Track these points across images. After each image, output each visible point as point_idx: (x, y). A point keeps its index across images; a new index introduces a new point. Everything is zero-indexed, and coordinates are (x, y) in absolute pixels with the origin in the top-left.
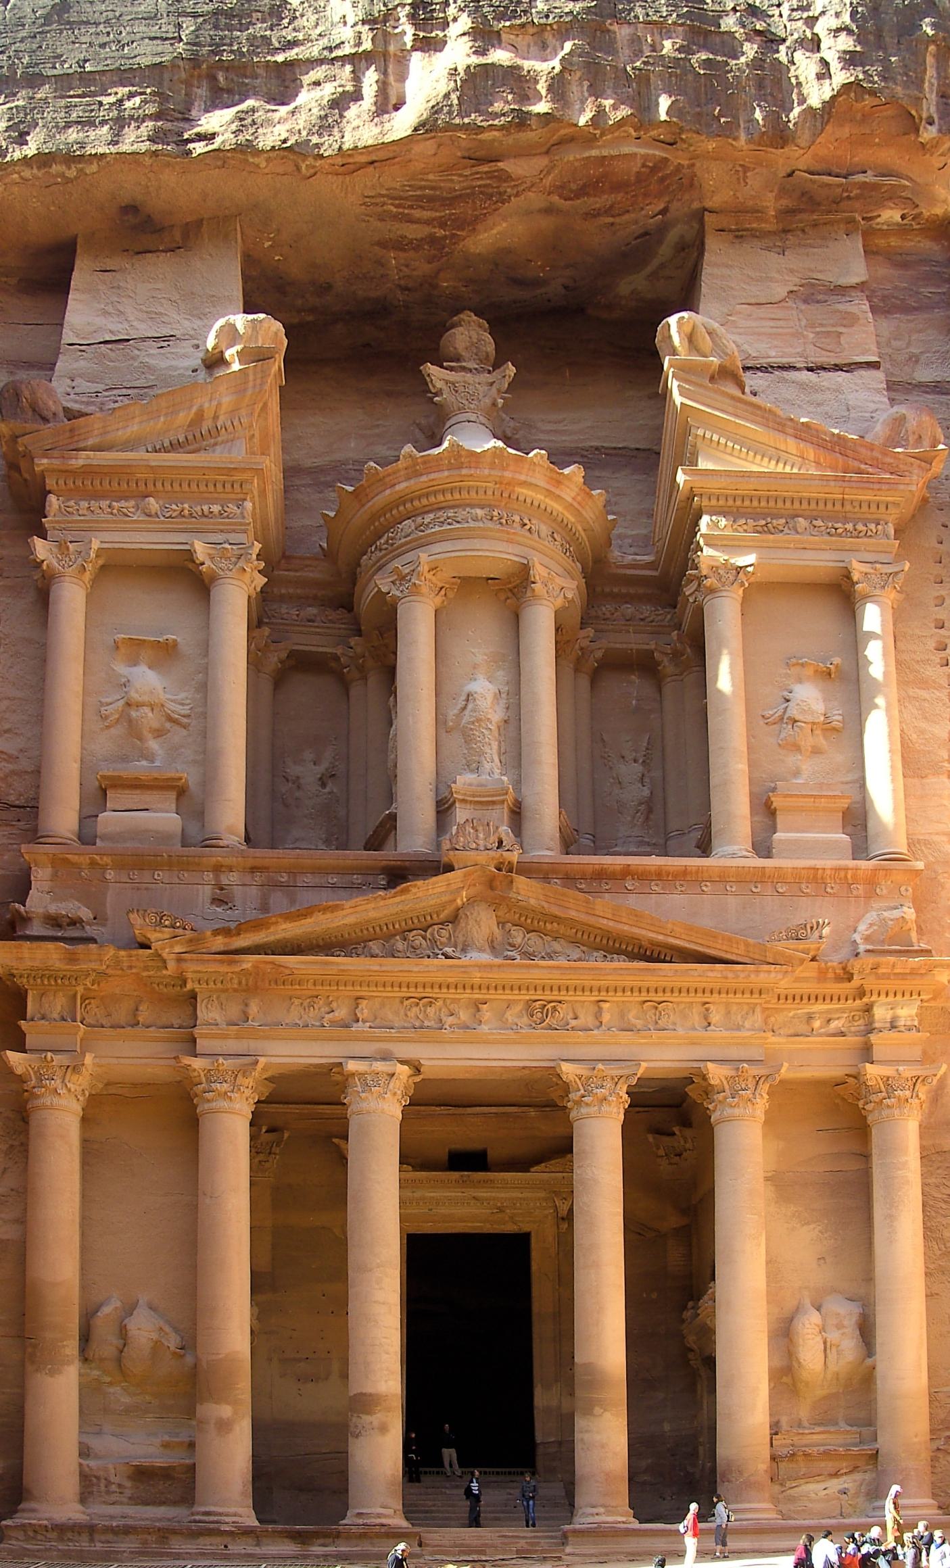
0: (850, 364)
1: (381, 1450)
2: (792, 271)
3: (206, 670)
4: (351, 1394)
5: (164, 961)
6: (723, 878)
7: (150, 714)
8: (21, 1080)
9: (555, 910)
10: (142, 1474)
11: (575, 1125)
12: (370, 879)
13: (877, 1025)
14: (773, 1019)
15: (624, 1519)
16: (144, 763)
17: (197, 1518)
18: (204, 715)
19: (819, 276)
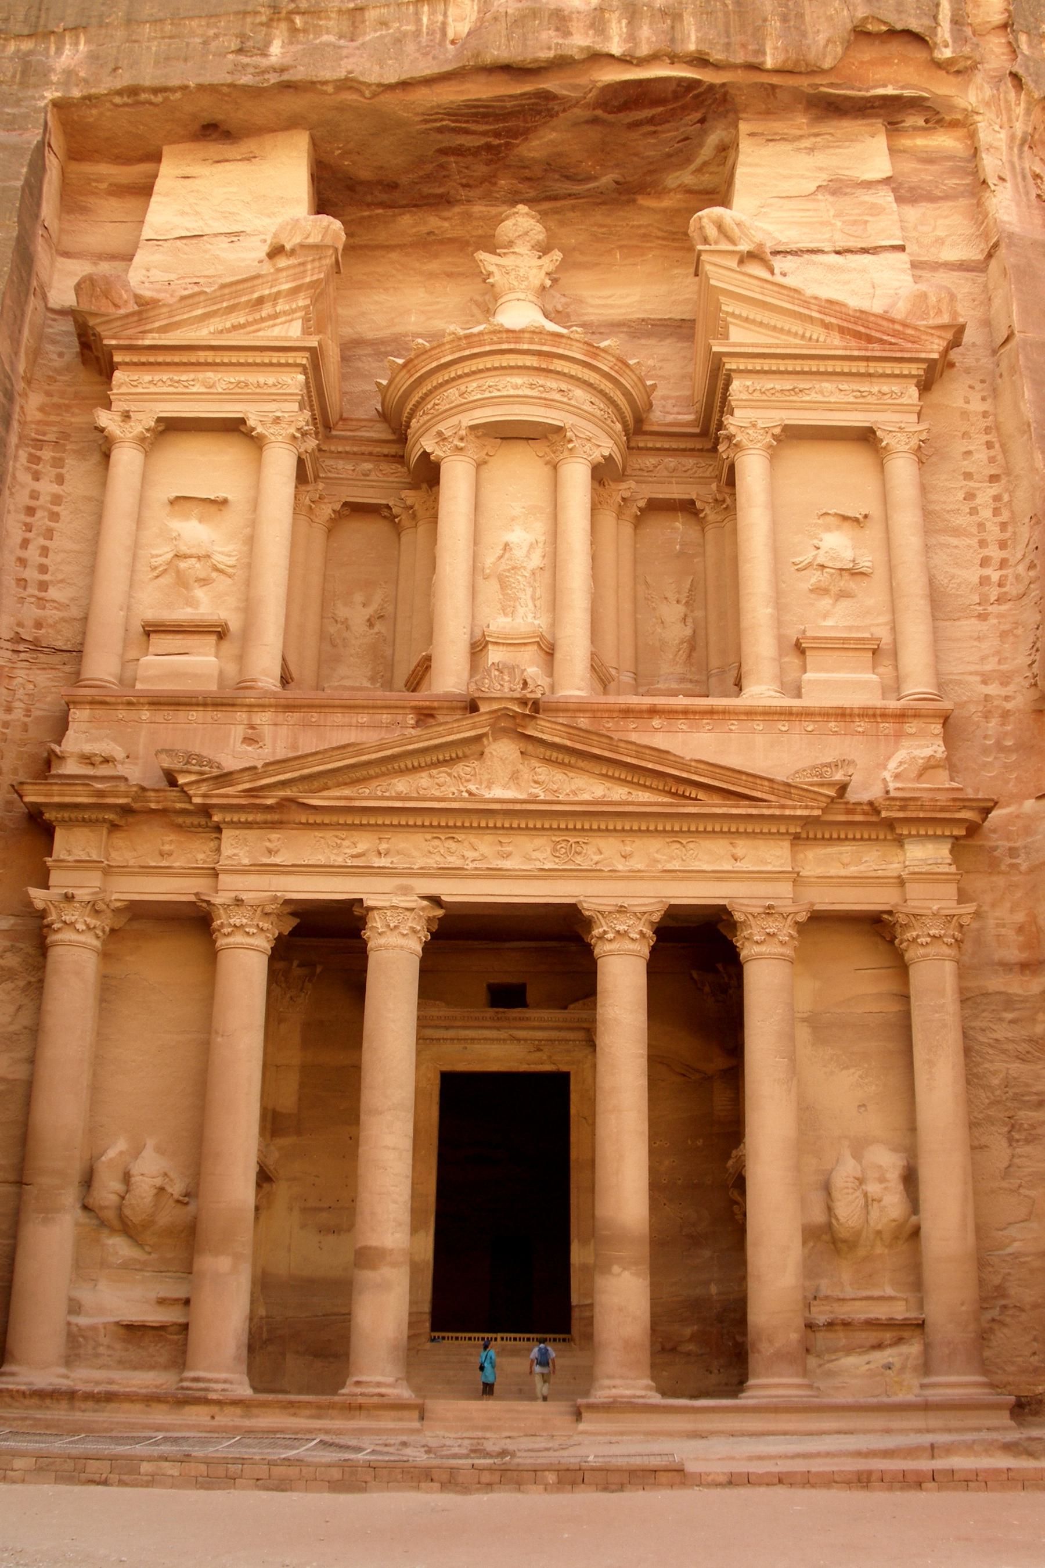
0: (876, 248)
1: (387, 1307)
2: (821, 169)
3: (253, 524)
4: (359, 1245)
5: (190, 798)
6: (751, 713)
7: (198, 565)
8: (43, 914)
9: (578, 746)
10: (133, 1331)
11: (599, 961)
12: (400, 718)
13: (907, 863)
14: (802, 856)
15: (643, 1393)
16: (189, 610)
17: (185, 1384)
18: (249, 566)
19: (847, 173)
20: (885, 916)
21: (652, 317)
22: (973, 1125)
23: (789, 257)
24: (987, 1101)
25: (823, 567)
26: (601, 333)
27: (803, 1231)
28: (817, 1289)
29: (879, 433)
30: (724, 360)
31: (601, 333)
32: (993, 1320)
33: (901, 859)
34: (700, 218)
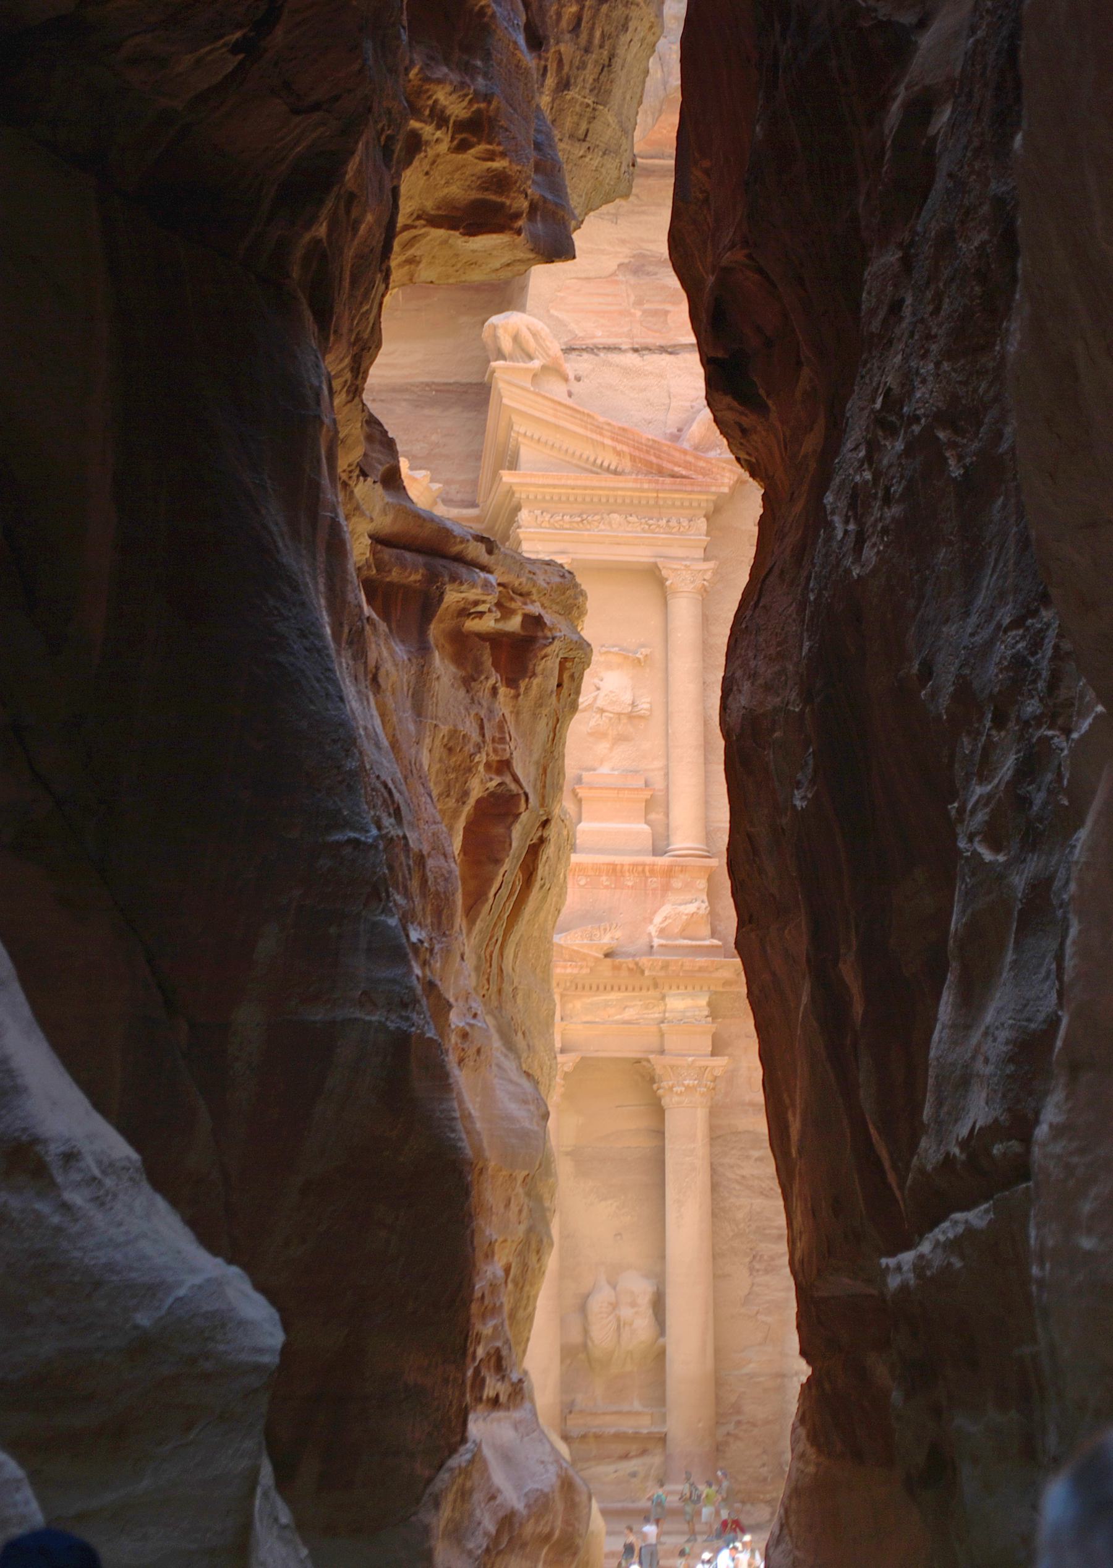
0: (675, 346)
14: (570, 1006)
20: (644, 1063)
21: (436, 380)
22: (716, 1256)
23: (585, 356)
24: (731, 1234)
25: (602, 711)
26: (382, 401)
27: (562, 1350)
28: (572, 1403)
29: (664, 573)
30: (514, 488)
31: (382, 401)
32: (728, 1434)
33: (662, 1008)
34: (495, 327)
